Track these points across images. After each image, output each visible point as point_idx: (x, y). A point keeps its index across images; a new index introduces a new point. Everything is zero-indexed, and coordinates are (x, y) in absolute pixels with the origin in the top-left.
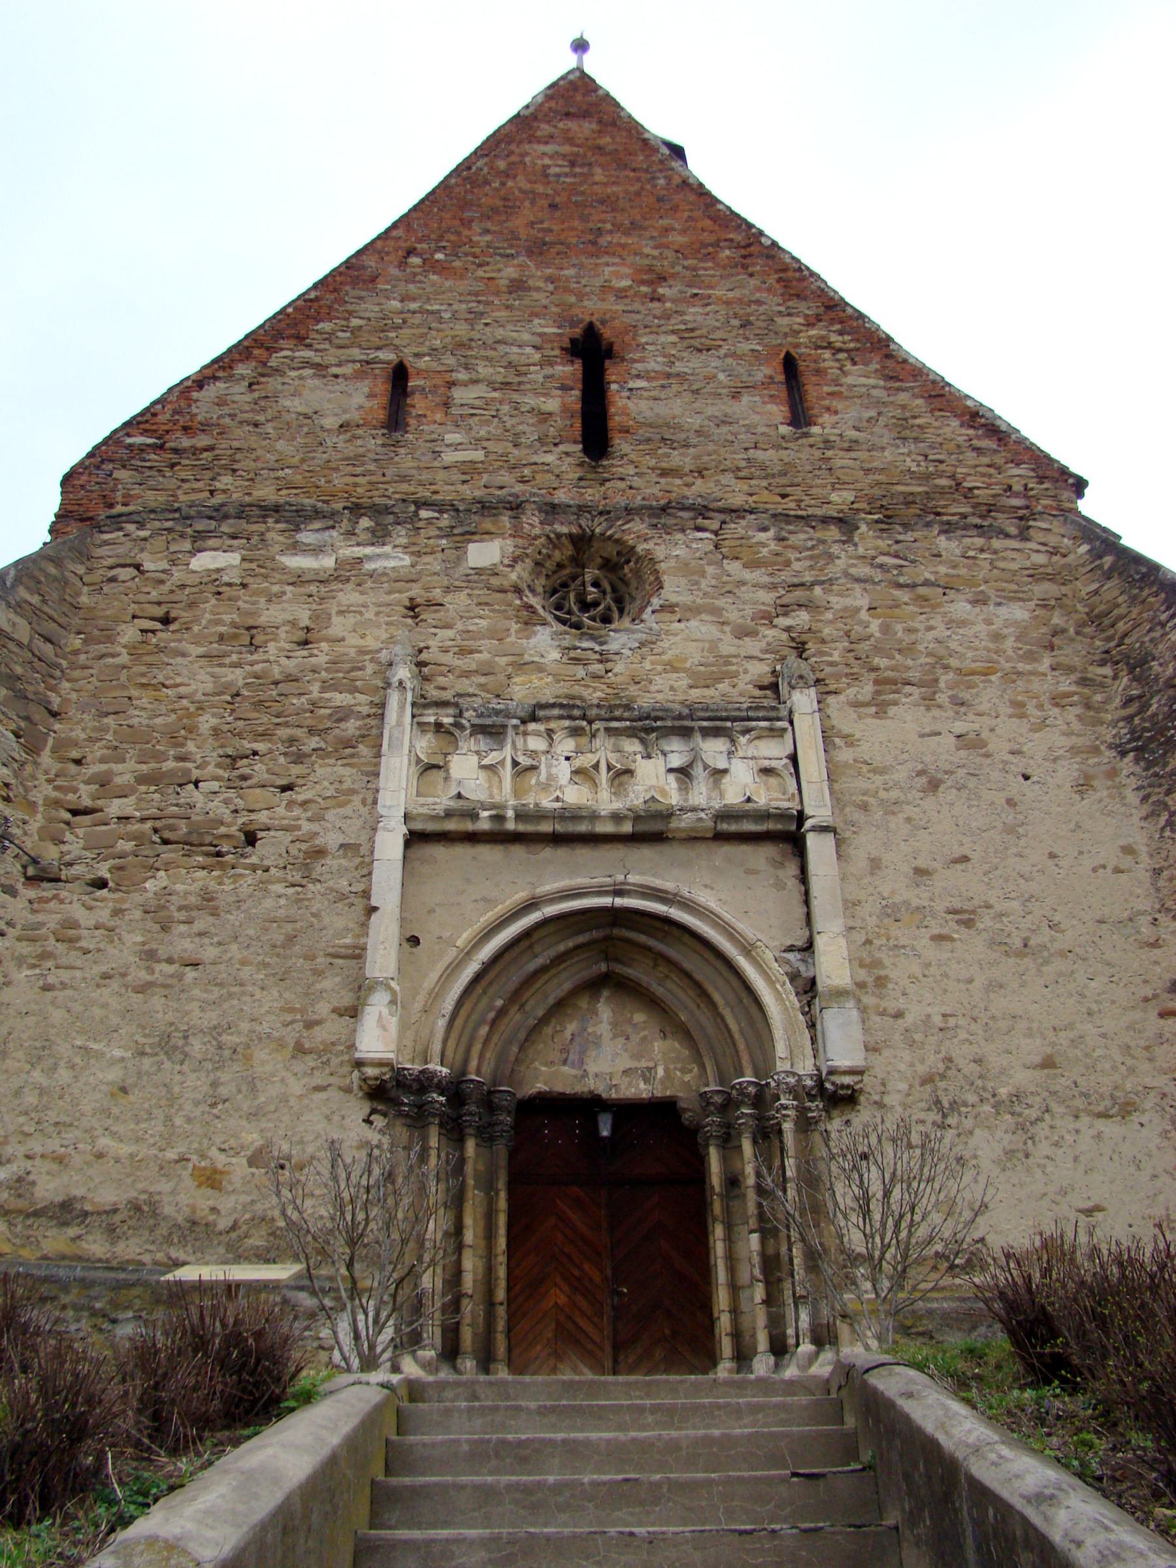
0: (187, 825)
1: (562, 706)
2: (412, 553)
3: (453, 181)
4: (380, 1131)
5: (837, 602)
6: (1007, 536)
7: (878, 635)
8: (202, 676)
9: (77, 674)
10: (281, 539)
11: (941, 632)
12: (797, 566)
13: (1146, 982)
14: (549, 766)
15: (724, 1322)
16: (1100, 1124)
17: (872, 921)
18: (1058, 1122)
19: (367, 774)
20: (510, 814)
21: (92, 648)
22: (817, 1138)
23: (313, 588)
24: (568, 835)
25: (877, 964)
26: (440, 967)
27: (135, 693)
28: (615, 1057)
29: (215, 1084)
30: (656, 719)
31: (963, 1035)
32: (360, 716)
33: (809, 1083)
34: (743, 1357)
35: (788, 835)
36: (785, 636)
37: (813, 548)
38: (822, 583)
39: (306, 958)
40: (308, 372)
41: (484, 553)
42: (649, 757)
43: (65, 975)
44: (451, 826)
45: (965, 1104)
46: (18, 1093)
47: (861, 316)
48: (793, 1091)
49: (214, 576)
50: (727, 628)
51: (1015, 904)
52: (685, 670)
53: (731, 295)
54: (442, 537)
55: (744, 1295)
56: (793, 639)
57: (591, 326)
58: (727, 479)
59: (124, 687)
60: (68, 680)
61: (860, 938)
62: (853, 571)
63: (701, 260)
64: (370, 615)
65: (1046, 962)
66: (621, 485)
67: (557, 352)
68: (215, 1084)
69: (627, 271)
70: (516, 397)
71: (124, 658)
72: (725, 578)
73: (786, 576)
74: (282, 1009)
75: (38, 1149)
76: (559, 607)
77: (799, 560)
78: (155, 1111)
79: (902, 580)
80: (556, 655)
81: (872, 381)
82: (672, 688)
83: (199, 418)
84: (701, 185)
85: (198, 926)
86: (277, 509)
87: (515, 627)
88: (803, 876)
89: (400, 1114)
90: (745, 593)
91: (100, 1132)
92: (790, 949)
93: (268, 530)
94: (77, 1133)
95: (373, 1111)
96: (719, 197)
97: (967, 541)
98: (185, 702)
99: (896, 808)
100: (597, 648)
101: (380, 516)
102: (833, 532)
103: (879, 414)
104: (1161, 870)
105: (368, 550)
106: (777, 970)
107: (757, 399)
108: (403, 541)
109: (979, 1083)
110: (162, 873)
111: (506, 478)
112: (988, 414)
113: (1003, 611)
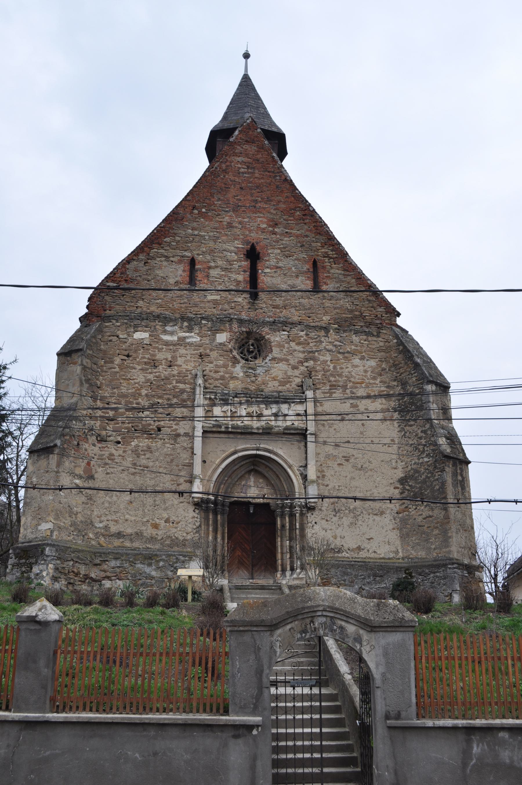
0: (142, 425)
1: (244, 394)
2: (200, 336)
3: (207, 174)
4: (197, 514)
5: (322, 358)
6: (373, 335)
7: (332, 370)
8: (141, 377)
9: (103, 374)
10: (160, 328)
11: (350, 369)
12: (311, 345)
13: (392, 479)
14: (240, 411)
15: (279, 562)
16: (375, 517)
17: (323, 459)
18: (364, 516)
19: (190, 411)
20: (230, 426)
21: (107, 365)
22: (305, 518)
23: (171, 347)
24: (246, 433)
25: (323, 471)
26: (212, 469)
27: (122, 381)
28: (254, 491)
29: (155, 501)
30: (269, 398)
31: (343, 492)
32: (187, 392)
33: (303, 504)
34: (284, 571)
35: (302, 435)
36: (306, 369)
37: (316, 338)
38: (318, 351)
39: (177, 466)
40: (163, 259)
41: (222, 338)
42: (267, 409)
43: (112, 470)
44: (214, 429)
45: (342, 510)
46: (103, 503)
47: (339, 244)
48: (300, 506)
49: (142, 341)
50: (290, 366)
51: (360, 455)
52: (277, 380)
53: (298, 232)
54: (208, 331)
55: (284, 555)
56: (308, 370)
57: (253, 244)
58: (293, 310)
59: (118, 379)
60: (102, 376)
61: (319, 464)
62: (327, 347)
63: (290, 217)
64: (188, 358)
65: (367, 472)
66: (261, 311)
67: (242, 256)
68: (155, 501)
69: (265, 220)
70: (230, 275)
71: (117, 369)
72: (290, 349)
73: (308, 348)
74: (171, 480)
75: (110, 518)
76: (242, 353)
77: (312, 342)
78: (140, 508)
79: (341, 351)
80: (242, 374)
81: (340, 272)
82: (274, 386)
83: (130, 276)
84: (291, 181)
85: (147, 456)
86: (158, 316)
87: (230, 364)
88: (306, 446)
89: (202, 509)
90: (296, 354)
91: (126, 514)
92: (301, 467)
93: (157, 325)
94: (120, 514)
95: (195, 508)
96: (298, 187)
97: (361, 337)
98: (137, 385)
99: (331, 426)
100: (253, 372)
101: (190, 322)
102: (323, 333)
103: (341, 285)
104: (400, 447)
105: (187, 334)
106: (298, 473)
107: (304, 278)
108: (197, 331)
109: (346, 505)
110: (136, 440)
111: (226, 306)
112: (374, 287)
113: (368, 362)
